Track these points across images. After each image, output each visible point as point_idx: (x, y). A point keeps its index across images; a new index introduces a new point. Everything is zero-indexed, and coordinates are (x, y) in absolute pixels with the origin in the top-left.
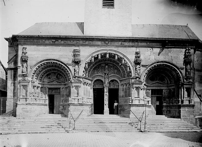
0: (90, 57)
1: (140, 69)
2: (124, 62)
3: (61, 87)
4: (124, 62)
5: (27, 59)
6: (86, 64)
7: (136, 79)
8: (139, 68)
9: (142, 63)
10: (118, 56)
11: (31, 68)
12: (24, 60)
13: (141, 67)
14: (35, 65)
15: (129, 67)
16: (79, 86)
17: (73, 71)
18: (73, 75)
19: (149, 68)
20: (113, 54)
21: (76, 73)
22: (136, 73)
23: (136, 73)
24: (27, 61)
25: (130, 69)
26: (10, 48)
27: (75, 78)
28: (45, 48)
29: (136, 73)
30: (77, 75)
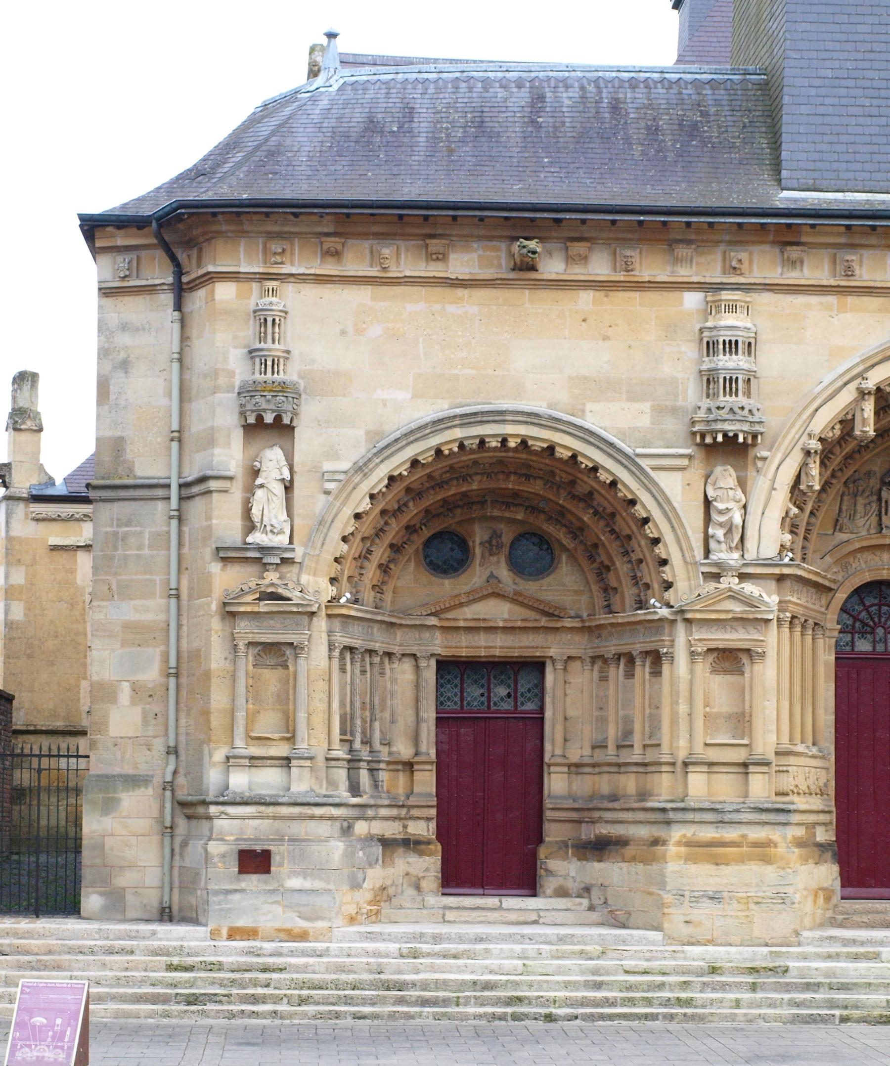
0: (847, 396)
3: (552, 652)
5: (295, 414)
6: (808, 453)
11: (327, 493)
12: (269, 418)
14: (362, 469)
16: (748, 651)
17: (693, 519)
24: (290, 429)
26: (109, 301)
27: (717, 577)
28: (451, 309)
30: (733, 558)
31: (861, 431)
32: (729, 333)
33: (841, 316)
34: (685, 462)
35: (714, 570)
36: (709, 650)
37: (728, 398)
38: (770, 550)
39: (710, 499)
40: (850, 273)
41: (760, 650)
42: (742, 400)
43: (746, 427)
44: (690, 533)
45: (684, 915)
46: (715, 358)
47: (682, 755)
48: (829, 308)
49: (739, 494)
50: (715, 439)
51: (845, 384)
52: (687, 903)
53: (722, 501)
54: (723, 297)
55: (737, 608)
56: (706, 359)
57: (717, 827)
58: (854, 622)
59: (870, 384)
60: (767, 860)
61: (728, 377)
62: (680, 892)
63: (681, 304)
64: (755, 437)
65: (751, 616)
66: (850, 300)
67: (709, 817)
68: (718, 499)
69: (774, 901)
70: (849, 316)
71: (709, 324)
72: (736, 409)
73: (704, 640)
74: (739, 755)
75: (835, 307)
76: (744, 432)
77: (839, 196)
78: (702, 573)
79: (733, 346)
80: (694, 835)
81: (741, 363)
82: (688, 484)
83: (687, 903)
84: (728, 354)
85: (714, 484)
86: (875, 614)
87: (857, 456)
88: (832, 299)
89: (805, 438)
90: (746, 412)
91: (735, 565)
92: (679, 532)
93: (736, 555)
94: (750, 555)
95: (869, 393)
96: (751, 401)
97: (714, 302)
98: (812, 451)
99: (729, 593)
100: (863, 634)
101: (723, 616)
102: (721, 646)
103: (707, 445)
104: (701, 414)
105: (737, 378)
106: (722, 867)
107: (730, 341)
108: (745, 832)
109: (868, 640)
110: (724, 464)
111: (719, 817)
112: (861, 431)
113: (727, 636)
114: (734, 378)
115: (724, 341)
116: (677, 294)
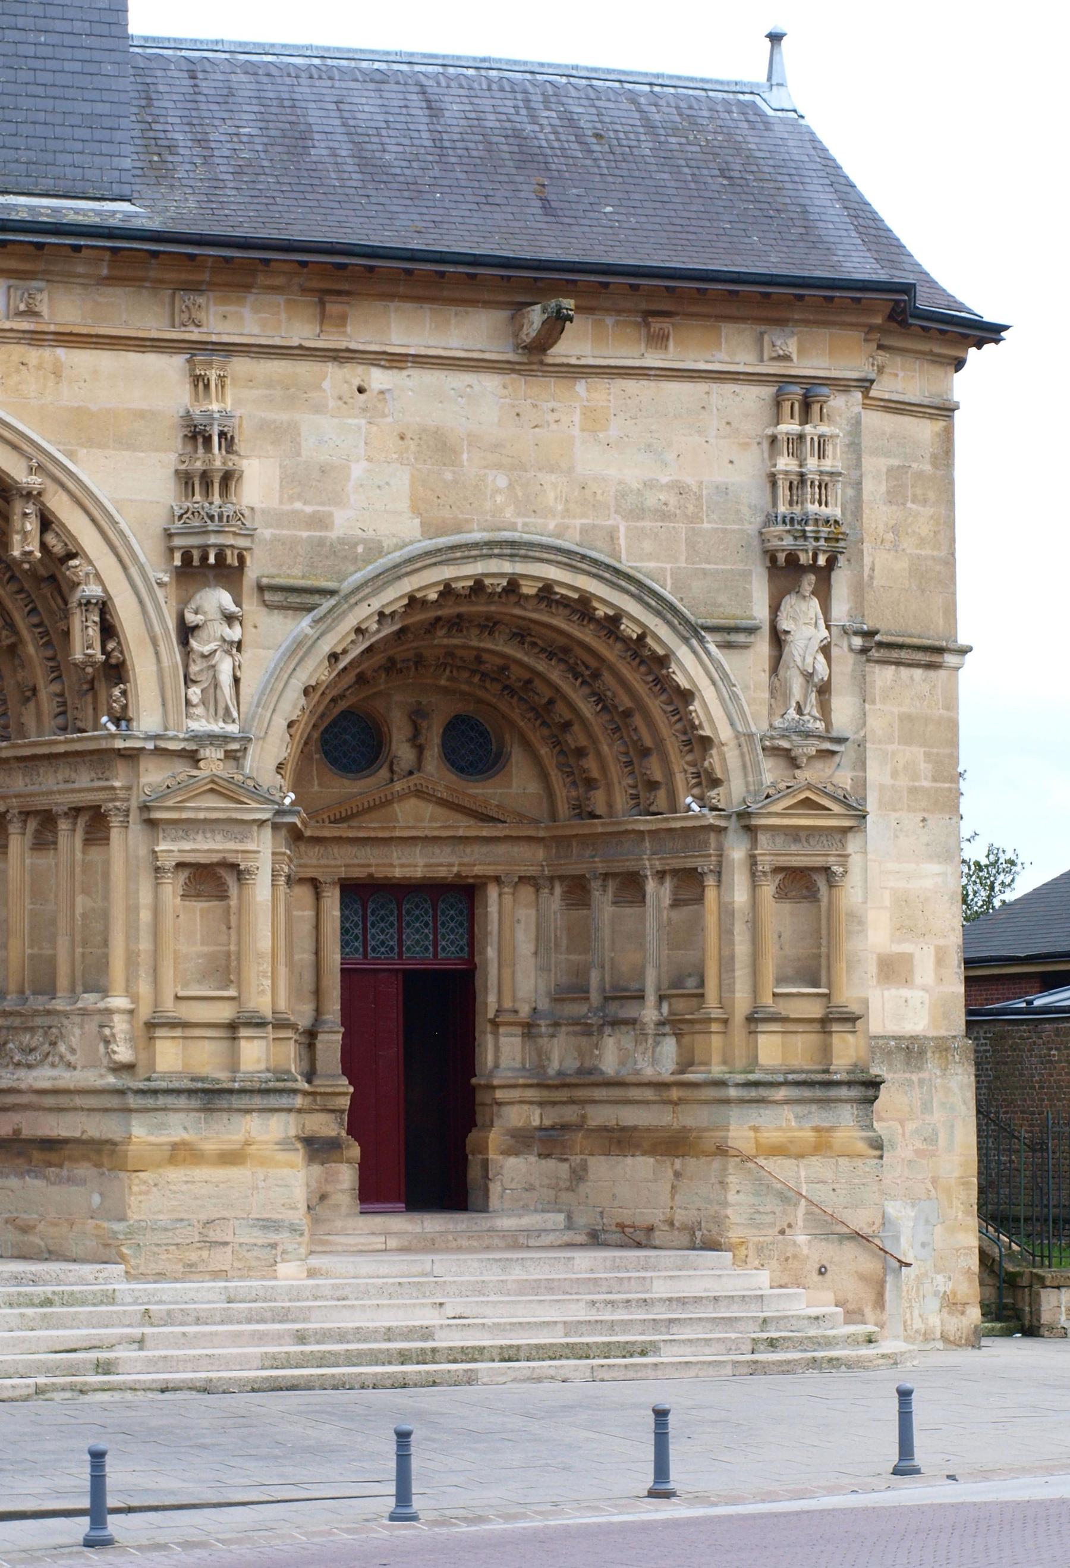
1: (235, 633)
2: (34, 547)
4: (43, 546)
7: (192, 758)
8: (230, 619)
9: (253, 573)
13: (251, 606)
15: (104, 607)
19: (351, 621)
22: (188, 681)
23: (195, 693)
25: (108, 630)
29: (188, 681)
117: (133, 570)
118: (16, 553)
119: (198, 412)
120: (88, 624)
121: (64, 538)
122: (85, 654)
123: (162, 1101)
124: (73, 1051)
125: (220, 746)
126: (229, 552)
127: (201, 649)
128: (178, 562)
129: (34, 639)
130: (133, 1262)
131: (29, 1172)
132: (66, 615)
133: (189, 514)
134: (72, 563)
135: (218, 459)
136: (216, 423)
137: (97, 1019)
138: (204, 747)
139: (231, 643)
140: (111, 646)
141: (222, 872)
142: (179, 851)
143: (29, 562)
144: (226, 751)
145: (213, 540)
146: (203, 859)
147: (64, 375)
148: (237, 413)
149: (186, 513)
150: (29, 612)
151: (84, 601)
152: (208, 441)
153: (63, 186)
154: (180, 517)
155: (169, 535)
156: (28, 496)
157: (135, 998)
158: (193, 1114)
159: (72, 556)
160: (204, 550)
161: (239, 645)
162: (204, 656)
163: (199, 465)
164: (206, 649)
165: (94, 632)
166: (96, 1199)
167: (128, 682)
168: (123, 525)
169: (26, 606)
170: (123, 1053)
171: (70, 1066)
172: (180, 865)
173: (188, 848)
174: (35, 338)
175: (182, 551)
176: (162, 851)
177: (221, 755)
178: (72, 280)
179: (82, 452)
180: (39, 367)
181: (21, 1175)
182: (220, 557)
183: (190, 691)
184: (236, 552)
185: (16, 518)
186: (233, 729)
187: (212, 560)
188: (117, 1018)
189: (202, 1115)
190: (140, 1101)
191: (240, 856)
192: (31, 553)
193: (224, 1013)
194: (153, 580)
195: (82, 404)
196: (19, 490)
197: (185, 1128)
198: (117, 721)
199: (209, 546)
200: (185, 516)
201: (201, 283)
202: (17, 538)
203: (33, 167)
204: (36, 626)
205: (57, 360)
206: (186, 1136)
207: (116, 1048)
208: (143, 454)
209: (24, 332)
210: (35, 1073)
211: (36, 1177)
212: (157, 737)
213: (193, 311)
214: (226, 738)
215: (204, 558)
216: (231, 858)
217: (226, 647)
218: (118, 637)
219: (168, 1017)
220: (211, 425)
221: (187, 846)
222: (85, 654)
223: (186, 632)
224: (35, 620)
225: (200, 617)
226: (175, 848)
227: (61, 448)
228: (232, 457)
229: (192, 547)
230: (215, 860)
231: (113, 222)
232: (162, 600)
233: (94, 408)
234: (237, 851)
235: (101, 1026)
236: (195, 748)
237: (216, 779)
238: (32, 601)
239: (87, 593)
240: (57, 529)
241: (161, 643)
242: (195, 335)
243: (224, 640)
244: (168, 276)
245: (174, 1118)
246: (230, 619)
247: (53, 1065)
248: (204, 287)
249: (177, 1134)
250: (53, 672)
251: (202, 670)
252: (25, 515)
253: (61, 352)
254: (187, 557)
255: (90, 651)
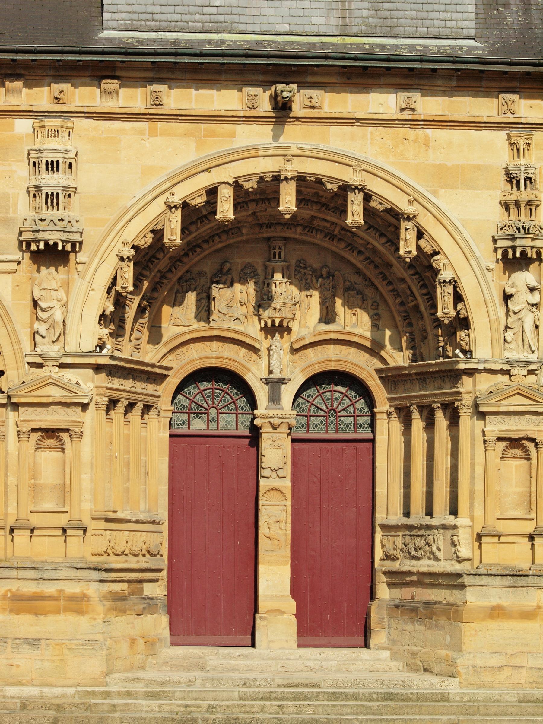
1: (535, 298)
4: (418, 248)
8: (532, 290)
10: (368, 197)
15: (455, 283)
16: (67, 430)
18: (27, 346)
20: (333, 180)
21: (42, 328)
22: (507, 328)
23: (509, 335)
25: (458, 298)
31: (169, 239)
32: (51, 155)
33: (152, 139)
34: (14, 266)
35: (38, 360)
36: (34, 430)
37: (50, 211)
38: (89, 345)
39: (36, 299)
40: (157, 103)
41: (77, 430)
42: (61, 213)
43: (65, 237)
44: (18, 328)
45: (7, 659)
46: (39, 177)
47: (11, 522)
48: (141, 132)
49: (61, 294)
50: (38, 246)
51: (155, 198)
52: (9, 649)
53: (46, 300)
54: (46, 124)
55: (56, 393)
56: (33, 177)
57: (38, 583)
58: (191, 404)
59: (176, 200)
60: (80, 612)
61: (50, 194)
62: (4, 640)
63: (13, 129)
64: (73, 245)
65: (68, 401)
66: (160, 125)
67: (31, 574)
68: (42, 298)
69: (86, 647)
70: (158, 140)
71: (36, 147)
72: (56, 221)
73: (29, 421)
74: (62, 521)
75: (147, 131)
76: (63, 241)
77: (153, 35)
78: (28, 363)
79: (55, 166)
80: (18, 590)
81: (61, 181)
82: (18, 286)
83: (9, 649)
84: (50, 173)
85: (39, 285)
86: (209, 396)
87: (185, 259)
88: (143, 125)
89: (120, 245)
90: (65, 222)
91: (55, 356)
92: (8, 327)
93: (57, 347)
94: (71, 348)
95: (175, 207)
96: (70, 214)
97: (40, 127)
98: (125, 257)
99: (50, 381)
100: (198, 415)
101: (44, 400)
102: (43, 427)
103: (32, 252)
104: (28, 225)
105: (57, 194)
106: (42, 617)
107: (52, 162)
108: (63, 588)
109: (203, 419)
110: (48, 268)
111: (40, 574)
112: (169, 239)
113: (49, 418)
114: (55, 194)
115: (47, 162)
116: (9, 120)
117: (473, 262)
118: (401, 252)
119: (512, 166)
120: (445, 294)
121: (431, 243)
122: (443, 312)
123: (485, 580)
124: (439, 549)
125: (524, 367)
126: (529, 250)
127: (513, 309)
128: (500, 256)
129: (424, 301)
130: (464, 676)
131: (417, 621)
132: (435, 288)
133: (507, 227)
134: (436, 258)
135: (525, 195)
136: (522, 172)
137: (450, 532)
138: (513, 367)
139: (533, 305)
140: (460, 306)
141: (524, 442)
142: (499, 431)
143: (410, 258)
144: (528, 370)
145: (518, 242)
146: (513, 436)
147: (431, 145)
148: (537, 166)
149: (505, 226)
150: (421, 286)
151: (442, 281)
152: (518, 182)
153: (434, 31)
154: (501, 229)
155: (495, 241)
156: (409, 219)
157: (472, 519)
158: (504, 589)
159: (437, 253)
160: (514, 248)
161: (536, 305)
162: (515, 313)
163: (514, 198)
164: (516, 309)
165: (449, 300)
166: (448, 638)
167: (470, 329)
168: (466, 234)
169: (419, 282)
170: (464, 551)
171: (437, 559)
172: (499, 439)
173: (504, 429)
174: (414, 123)
175: (502, 249)
176: (488, 431)
177: (525, 372)
178: (435, 88)
179: (442, 191)
180: (416, 141)
181: (413, 622)
182: (523, 253)
183: (506, 334)
184: (535, 250)
185: (402, 231)
186: (533, 357)
187: (518, 255)
188: (460, 531)
189: (509, 589)
190: (472, 581)
191: (536, 433)
192: (410, 252)
193: (529, 527)
194: (484, 267)
195: (442, 162)
196: (403, 214)
197: (500, 598)
198: (464, 352)
199: (516, 247)
200: (504, 229)
201: (515, 88)
202: (402, 243)
203: (414, 21)
204: (425, 295)
205: (427, 136)
206: (499, 602)
207: (459, 549)
208: (480, 192)
209: (405, 120)
210: (421, 562)
211: (421, 625)
212: (485, 362)
213: (509, 104)
214: (530, 363)
215: (514, 253)
216: (531, 435)
217: (530, 307)
218: (464, 302)
219: (490, 531)
220: (520, 173)
221: (503, 427)
222: (443, 312)
223: (507, 297)
224: (424, 291)
225: (513, 289)
226: (496, 429)
227: (429, 189)
228: (534, 192)
229: (508, 247)
230: (521, 436)
231: (462, 53)
232: (490, 279)
233: (449, 164)
234: (534, 431)
235: (453, 536)
236: (509, 368)
237: (520, 387)
238: (423, 280)
239: (444, 276)
240: (426, 238)
241: (489, 305)
242: (511, 118)
243: (528, 304)
244: (493, 84)
245: (492, 590)
246: (532, 290)
247: (429, 558)
248: (518, 90)
249: (494, 601)
250: (435, 322)
251: (514, 321)
252: (406, 229)
253: (429, 131)
254: (505, 254)
255: (446, 311)
